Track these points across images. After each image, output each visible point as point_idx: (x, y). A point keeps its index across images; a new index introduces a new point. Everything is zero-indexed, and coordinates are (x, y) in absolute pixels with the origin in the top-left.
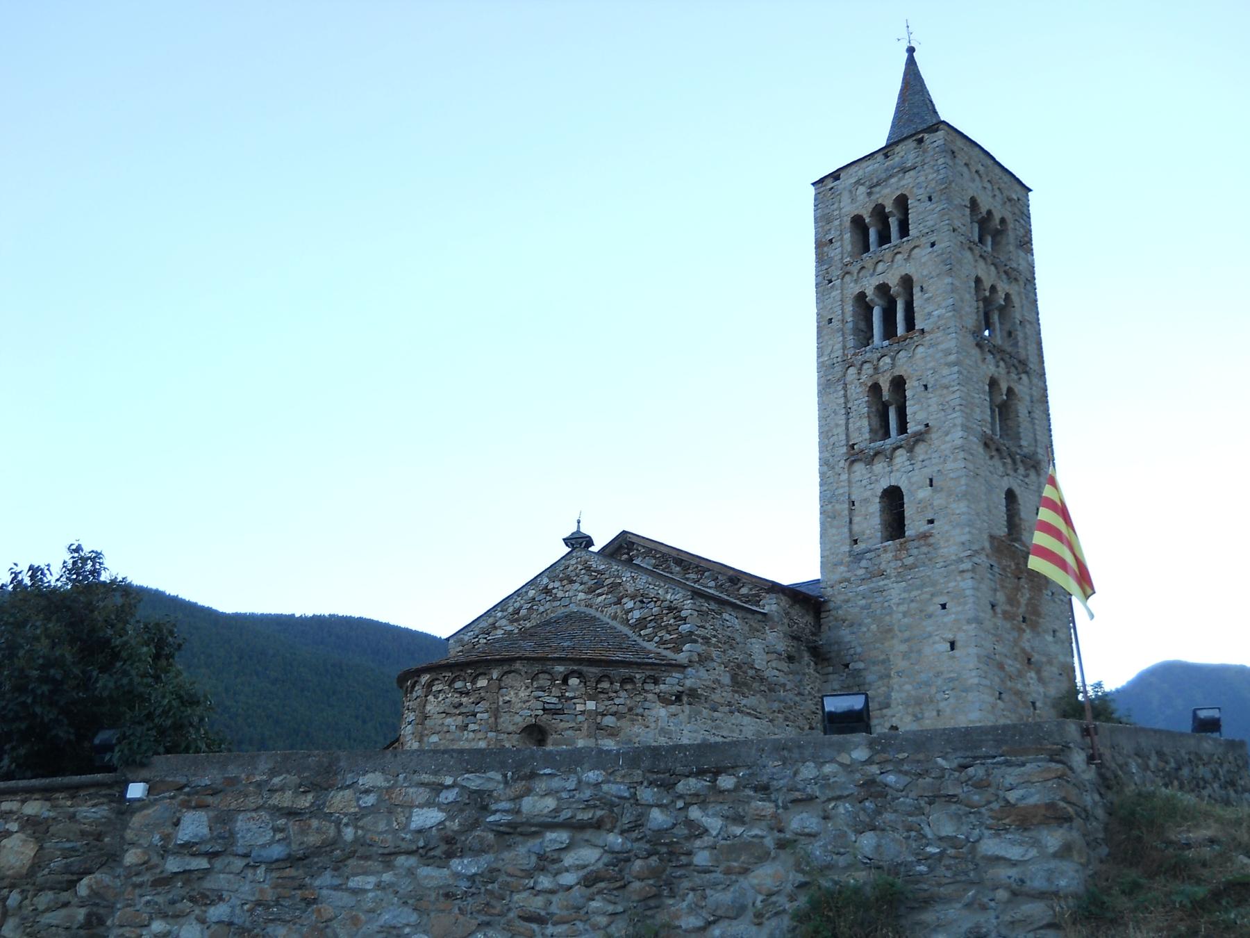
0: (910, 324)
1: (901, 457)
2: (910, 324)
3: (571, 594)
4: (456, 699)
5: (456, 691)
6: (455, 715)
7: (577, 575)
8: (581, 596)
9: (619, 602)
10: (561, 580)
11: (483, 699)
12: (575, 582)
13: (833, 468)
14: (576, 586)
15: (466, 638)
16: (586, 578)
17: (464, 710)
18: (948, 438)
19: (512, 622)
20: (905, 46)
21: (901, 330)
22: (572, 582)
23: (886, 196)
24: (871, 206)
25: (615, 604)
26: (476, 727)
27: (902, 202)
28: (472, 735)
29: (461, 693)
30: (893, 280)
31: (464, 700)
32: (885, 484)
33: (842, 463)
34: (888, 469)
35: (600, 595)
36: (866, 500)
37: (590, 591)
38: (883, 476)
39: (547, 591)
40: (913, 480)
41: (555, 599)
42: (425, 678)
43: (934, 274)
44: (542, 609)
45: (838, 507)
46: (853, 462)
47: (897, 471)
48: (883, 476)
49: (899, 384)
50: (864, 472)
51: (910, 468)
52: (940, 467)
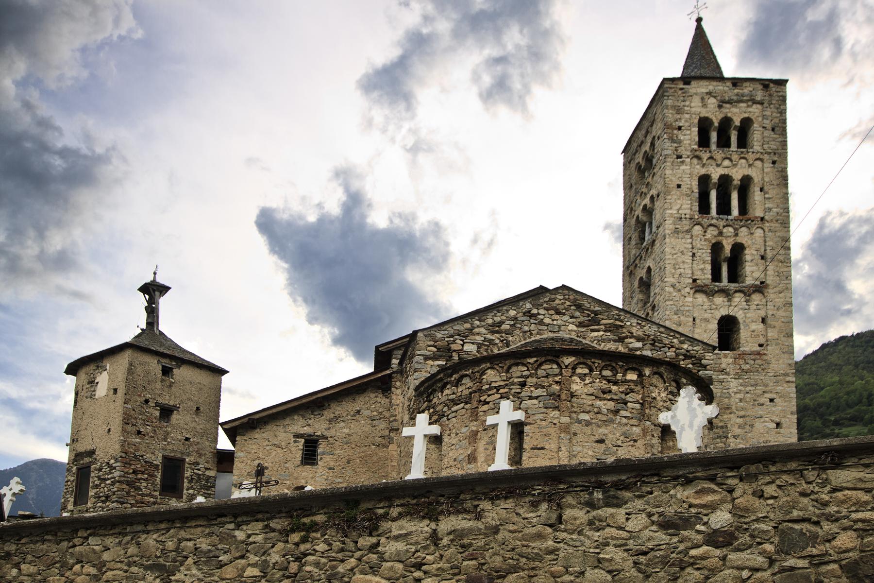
0: (744, 208)
1: (738, 298)
2: (744, 208)
3: (559, 322)
4: (604, 385)
5: (604, 378)
6: (605, 399)
7: (567, 309)
8: (572, 327)
9: (621, 340)
10: (547, 309)
11: (632, 391)
12: (564, 314)
13: (679, 291)
14: (566, 318)
15: (439, 335)
16: (577, 314)
17: (615, 397)
18: (781, 295)
19: (493, 332)
20: (695, 17)
21: (735, 212)
22: (558, 313)
23: (737, 114)
24: (720, 116)
25: (615, 341)
26: (629, 415)
27: (746, 123)
28: (624, 421)
29: (609, 381)
30: (737, 175)
31: (614, 388)
32: (724, 312)
33: (688, 290)
34: (726, 303)
35: (593, 331)
36: (707, 320)
37: (580, 325)
38: (721, 307)
39: (528, 314)
40: (748, 315)
41: (541, 323)
42: (568, 360)
43: (775, 183)
44: (526, 328)
45: (682, 318)
46: (696, 292)
47: (737, 307)
48: (721, 307)
49: (738, 249)
50: (706, 300)
51: (747, 307)
52: (774, 312)
